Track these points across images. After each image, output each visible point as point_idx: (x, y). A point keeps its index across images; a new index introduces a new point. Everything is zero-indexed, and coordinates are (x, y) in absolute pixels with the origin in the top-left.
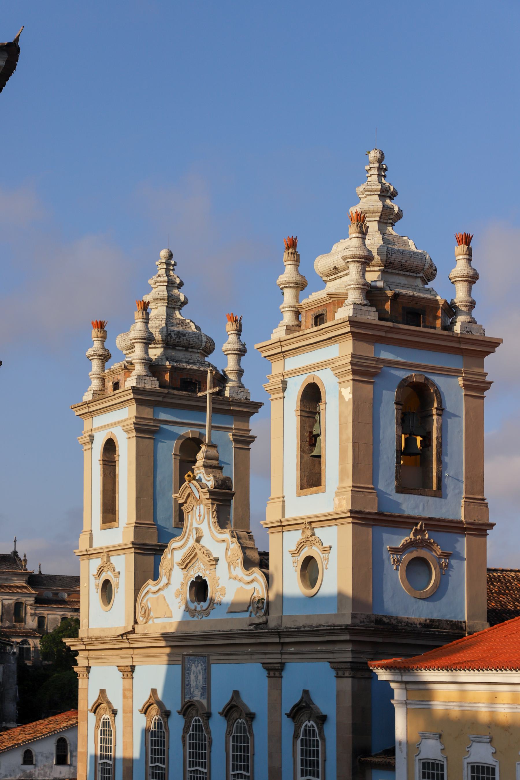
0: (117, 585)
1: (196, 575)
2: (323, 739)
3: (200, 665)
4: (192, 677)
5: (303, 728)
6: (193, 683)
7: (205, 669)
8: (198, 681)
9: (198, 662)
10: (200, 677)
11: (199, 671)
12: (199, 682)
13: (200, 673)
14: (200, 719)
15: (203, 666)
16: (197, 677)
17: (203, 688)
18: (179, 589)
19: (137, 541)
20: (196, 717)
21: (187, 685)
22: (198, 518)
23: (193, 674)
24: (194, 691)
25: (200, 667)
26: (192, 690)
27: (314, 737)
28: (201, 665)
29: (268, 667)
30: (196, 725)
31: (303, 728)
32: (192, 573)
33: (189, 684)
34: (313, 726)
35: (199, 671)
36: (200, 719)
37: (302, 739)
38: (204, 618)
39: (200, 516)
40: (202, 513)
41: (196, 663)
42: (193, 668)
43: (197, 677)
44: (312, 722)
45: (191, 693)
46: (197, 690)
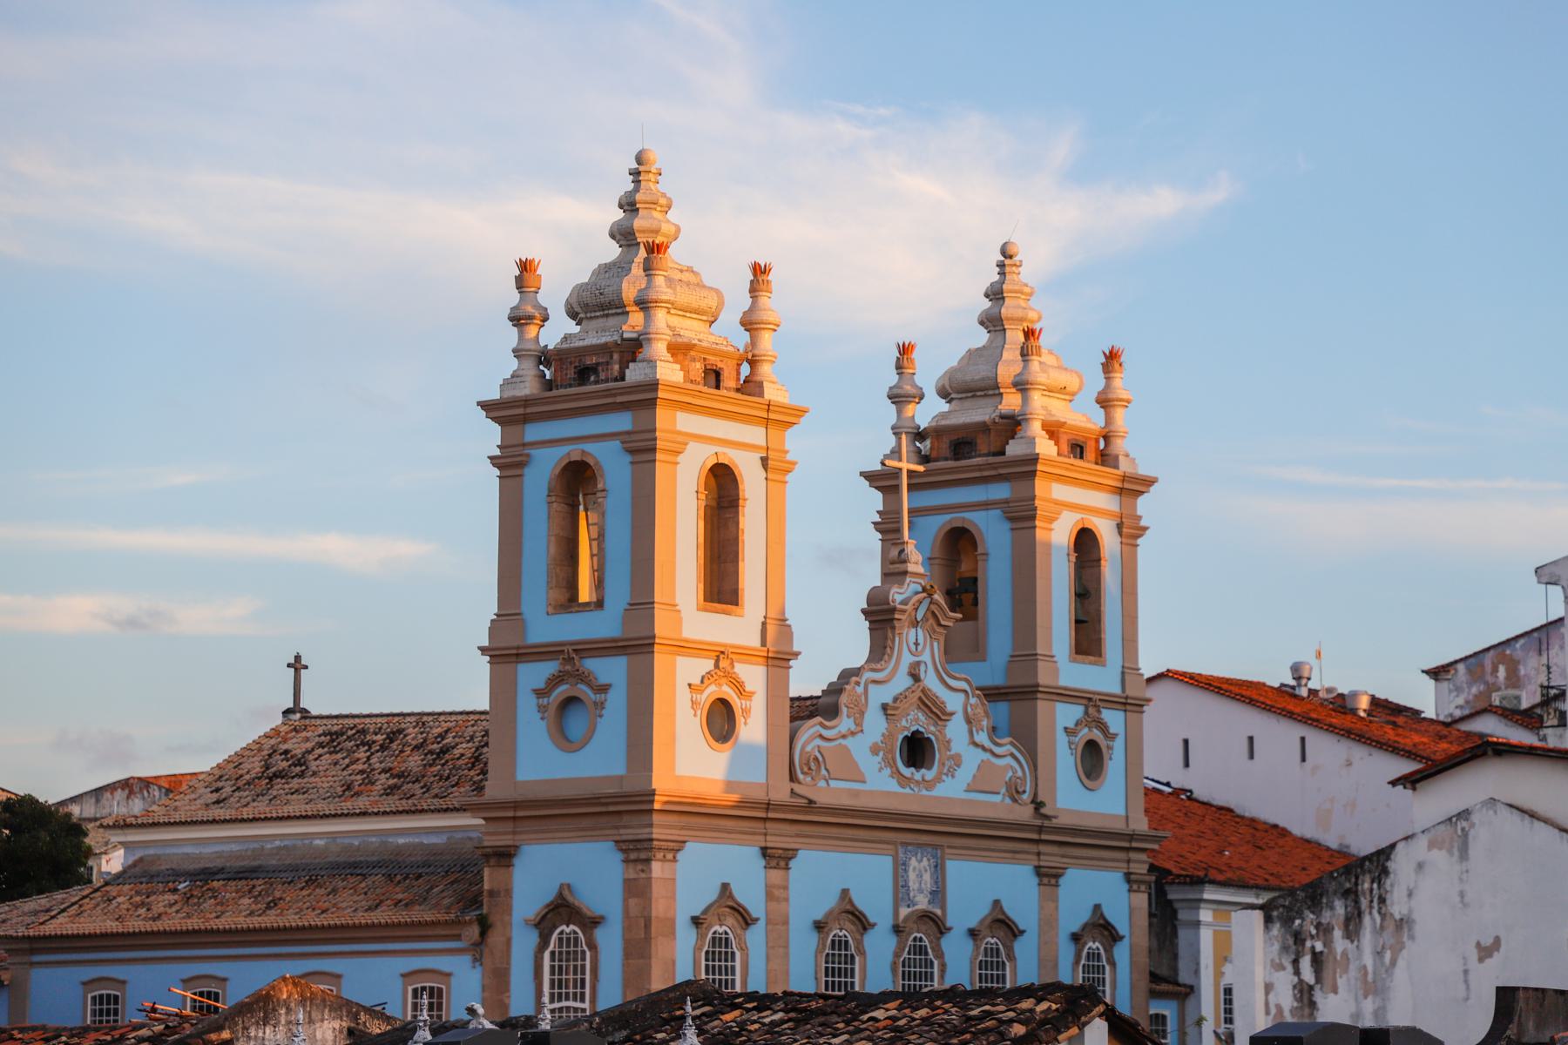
0: (746, 712)
1: (914, 729)
2: (1113, 964)
3: (925, 859)
4: (912, 875)
5: (1086, 951)
6: (914, 883)
7: (936, 866)
8: (923, 882)
9: (922, 854)
10: (927, 877)
11: (924, 867)
12: (926, 884)
13: (926, 871)
14: (923, 936)
15: (932, 861)
16: (921, 876)
17: (933, 893)
18: (876, 743)
19: (502, 613)
20: (915, 934)
21: (902, 887)
22: (913, 648)
23: (914, 869)
24: (914, 897)
25: (925, 862)
26: (912, 894)
27: (1098, 961)
28: (929, 860)
29: (1039, 872)
30: (915, 946)
31: (1086, 951)
32: (904, 723)
33: (906, 886)
34: (1098, 949)
35: (924, 867)
36: (923, 936)
37: (1084, 966)
38: (925, 792)
39: (917, 644)
40: (921, 640)
41: (919, 855)
42: (913, 862)
43: (920, 876)
44: (1097, 944)
45: (909, 899)
46: (922, 895)
